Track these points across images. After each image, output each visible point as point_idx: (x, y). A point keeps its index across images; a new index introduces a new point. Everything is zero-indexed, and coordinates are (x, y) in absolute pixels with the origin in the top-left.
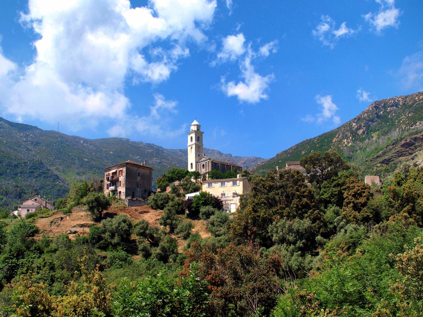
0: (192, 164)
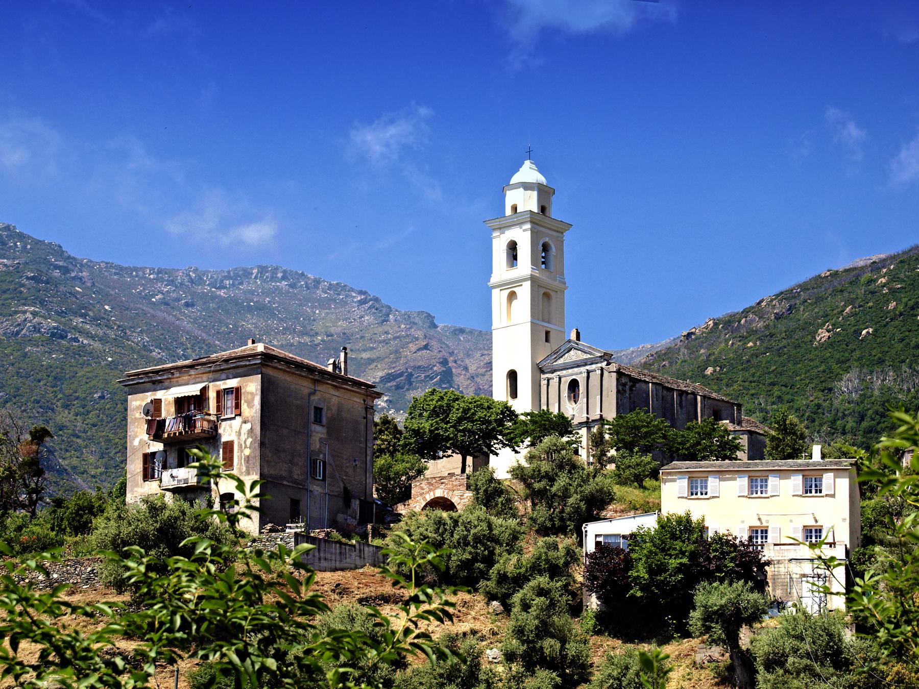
0: (512, 376)
